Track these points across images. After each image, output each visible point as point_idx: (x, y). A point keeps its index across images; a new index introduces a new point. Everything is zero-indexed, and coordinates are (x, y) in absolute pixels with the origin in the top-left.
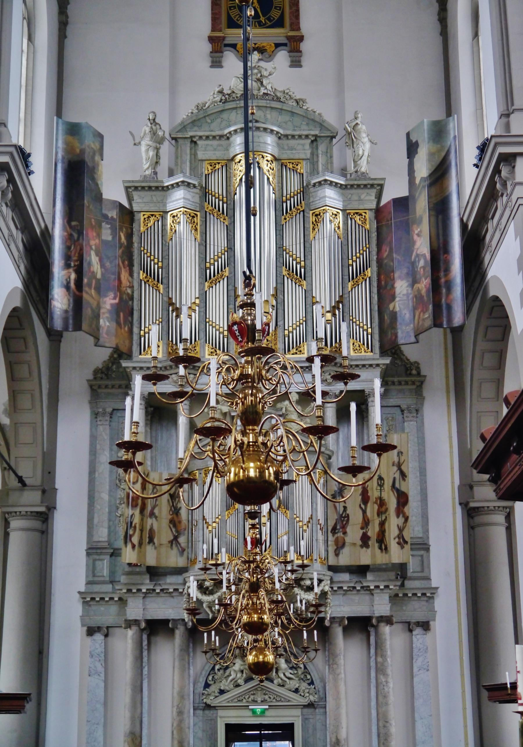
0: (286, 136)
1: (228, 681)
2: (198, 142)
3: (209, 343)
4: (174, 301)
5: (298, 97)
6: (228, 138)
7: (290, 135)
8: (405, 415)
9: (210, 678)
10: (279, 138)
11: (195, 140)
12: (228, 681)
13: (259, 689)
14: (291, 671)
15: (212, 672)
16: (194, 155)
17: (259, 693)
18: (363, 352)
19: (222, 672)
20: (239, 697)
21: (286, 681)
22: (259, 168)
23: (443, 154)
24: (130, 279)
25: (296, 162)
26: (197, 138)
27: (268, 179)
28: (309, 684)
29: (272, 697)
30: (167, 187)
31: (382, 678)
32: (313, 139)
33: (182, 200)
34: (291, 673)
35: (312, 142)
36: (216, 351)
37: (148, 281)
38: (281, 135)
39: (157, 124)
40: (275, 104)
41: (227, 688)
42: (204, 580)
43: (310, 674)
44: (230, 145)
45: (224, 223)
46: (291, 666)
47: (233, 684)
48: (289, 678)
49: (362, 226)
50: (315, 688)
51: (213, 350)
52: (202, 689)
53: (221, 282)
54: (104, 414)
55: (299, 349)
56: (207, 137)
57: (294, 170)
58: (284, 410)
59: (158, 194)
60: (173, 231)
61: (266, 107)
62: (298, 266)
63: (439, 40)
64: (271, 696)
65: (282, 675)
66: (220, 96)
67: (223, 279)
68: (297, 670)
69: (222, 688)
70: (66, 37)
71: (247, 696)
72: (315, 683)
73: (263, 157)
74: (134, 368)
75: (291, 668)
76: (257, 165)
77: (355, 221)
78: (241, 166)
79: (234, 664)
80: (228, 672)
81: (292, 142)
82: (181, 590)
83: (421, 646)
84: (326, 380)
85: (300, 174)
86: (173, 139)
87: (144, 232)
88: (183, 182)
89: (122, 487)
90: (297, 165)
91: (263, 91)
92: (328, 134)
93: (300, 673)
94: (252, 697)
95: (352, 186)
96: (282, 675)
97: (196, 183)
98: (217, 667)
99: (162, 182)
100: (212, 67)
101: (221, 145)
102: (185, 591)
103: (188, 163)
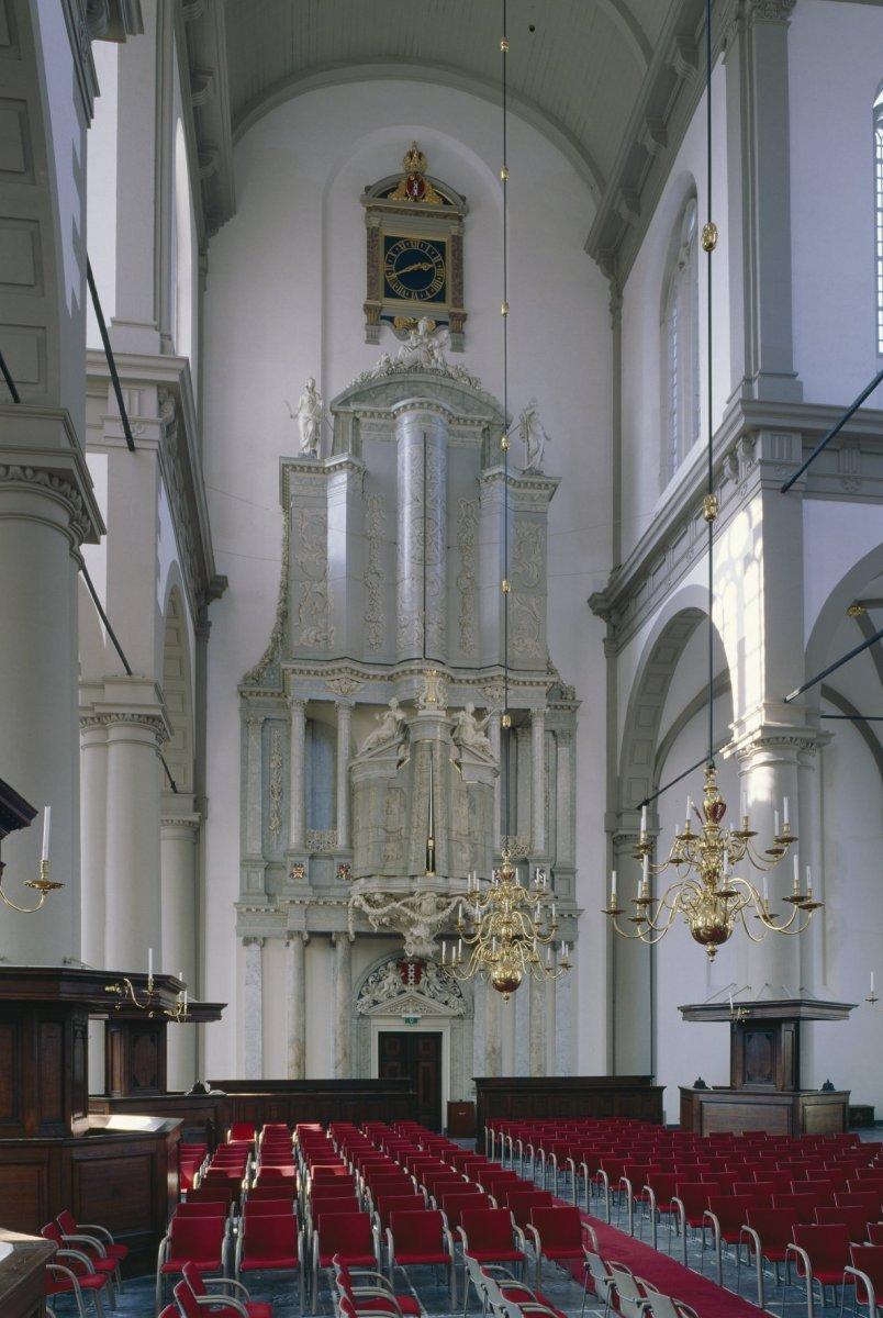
2: (363, 420)
6: (395, 417)
10: (450, 422)
11: (358, 416)
16: (356, 434)
26: (361, 413)
30: (329, 468)
32: (486, 426)
35: (484, 430)
39: (315, 394)
40: (448, 382)
42: (373, 894)
44: (395, 426)
56: (372, 413)
59: (318, 476)
61: (436, 384)
63: (608, 318)
70: (205, 289)
81: (462, 428)
86: (336, 414)
88: (347, 462)
91: (433, 365)
92: (503, 422)
101: (387, 426)
103: (350, 445)
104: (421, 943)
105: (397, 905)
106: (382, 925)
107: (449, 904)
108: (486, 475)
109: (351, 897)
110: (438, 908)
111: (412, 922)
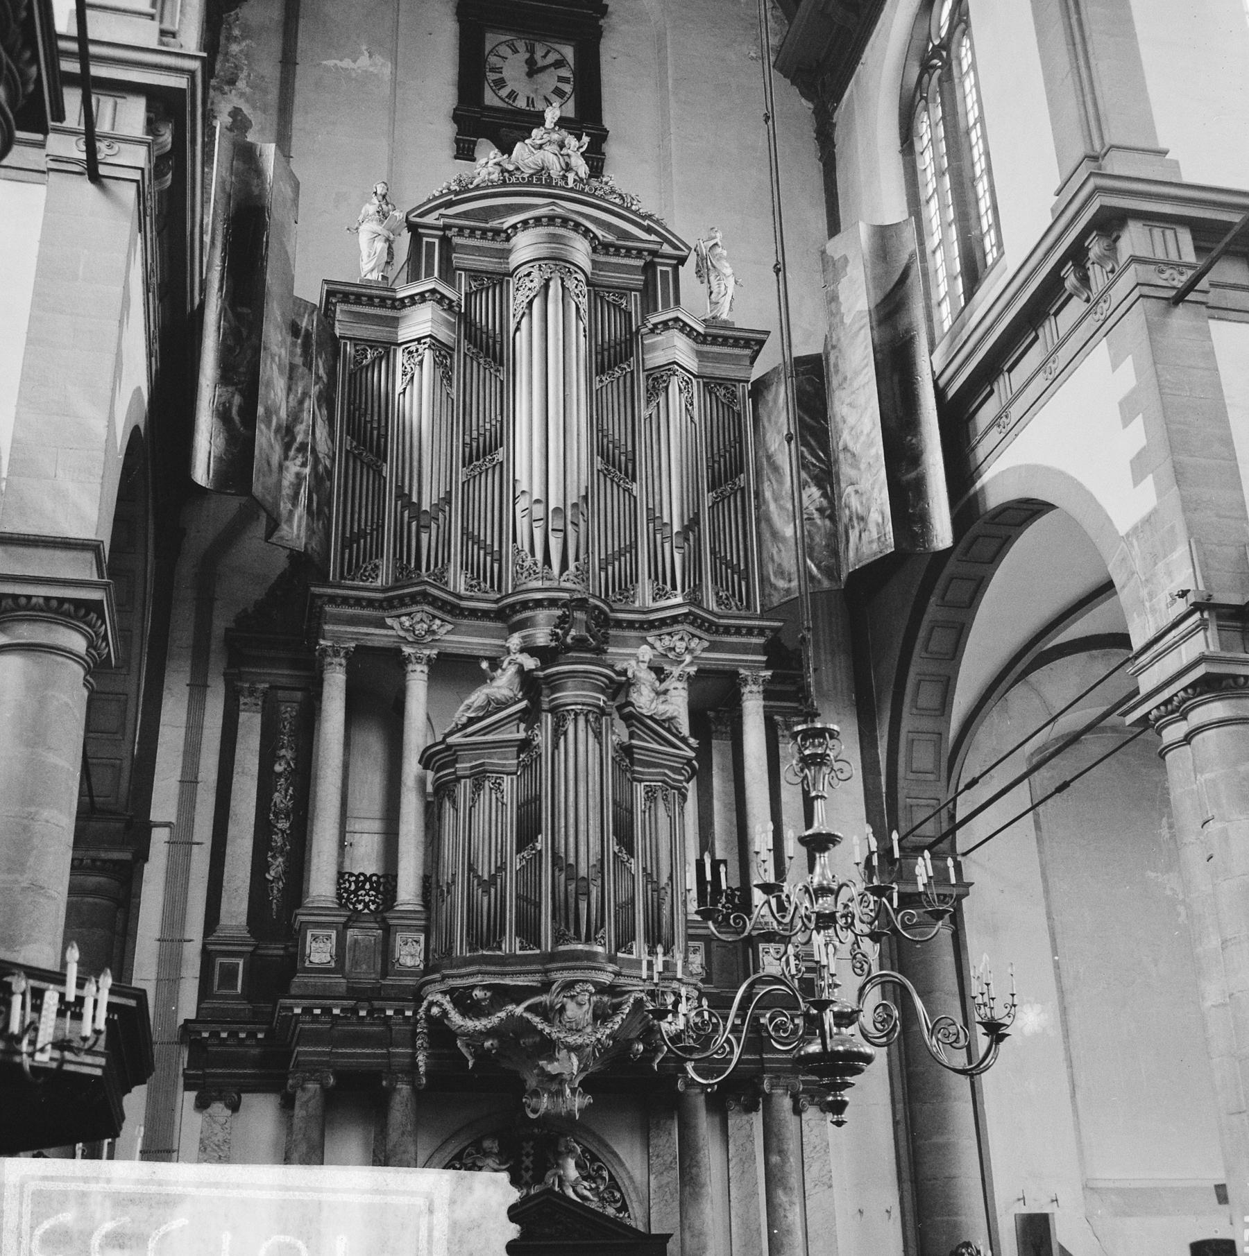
0: (606, 246)
2: (457, 240)
3: (467, 569)
4: (407, 491)
5: (623, 192)
6: (508, 239)
7: (612, 245)
8: (780, 733)
10: (594, 250)
11: (450, 234)
14: (586, 1184)
16: (446, 260)
18: (734, 608)
22: (563, 286)
23: (896, 277)
24: (329, 442)
25: (623, 291)
27: (578, 309)
28: (619, 1210)
30: (402, 300)
31: (781, 1196)
32: (649, 259)
33: (430, 324)
34: (585, 1188)
36: (479, 583)
37: (361, 454)
38: (600, 243)
42: (473, 987)
43: (619, 1190)
44: (510, 251)
45: (496, 376)
49: (729, 407)
50: (629, 1217)
51: (474, 582)
53: (490, 471)
54: (252, 692)
55: (626, 594)
57: (617, 307)
58: (630, 674)
60: (409, 376)
62: (623, 458)
66: (499, 168)
67: (494, 466)
68: (595, 1182)
72: (630, 1209)
73: (569, 271)
74: (332, 600)
75: (585, 1179)
76: (560, 282)
77: (717, 397)
78: (532, 281)
82: (409, 1013)
83: (818, 1141)
84: (673, 649)
85: (625, 312)
86: (413, 227)
87: (355, 374)
88: (433, 291)
89: (280, 826)
90: (621, 298)
93: (602, 1188)
95: (715, 337)
97: (454, 298)
99: (394, 291)
100: (456, 158)
102: (421, 1011)
104: (560, 1093)
105: (519, 1010)
106: (481, 1054)
107: (616, 1008)
108: (655, 319)
109: (423, 999)
110: (596, 1017)
111: (548, 1048)
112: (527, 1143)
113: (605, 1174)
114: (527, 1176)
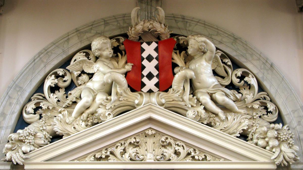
1: (74, 114)
9: (30, 107)
12: (74, 114)
13: (150, 132)
15: (35, 96)
17: (150, 141)
19: (60, 94)
20: (100, 150)
21: (217, 115)
29: (183, 153)
41: (70, 129)
46: (227, 82)
47: (86, 121)
48: (225, 108)
52: (9, 130)
64: (180, 149)
65: (205, 99)
69: (58, 129)
71: (120, 149)
79: (91, 76)
80: (74, 93)
94: (131, 151)
96: (205, 99)
98: (50, 82)
112: (149, 44)
113: (253, 81)
114: (150, 84)
